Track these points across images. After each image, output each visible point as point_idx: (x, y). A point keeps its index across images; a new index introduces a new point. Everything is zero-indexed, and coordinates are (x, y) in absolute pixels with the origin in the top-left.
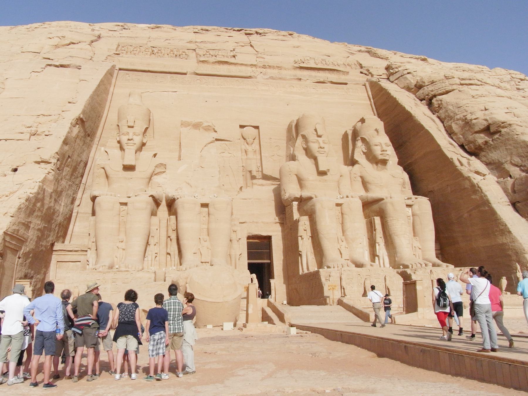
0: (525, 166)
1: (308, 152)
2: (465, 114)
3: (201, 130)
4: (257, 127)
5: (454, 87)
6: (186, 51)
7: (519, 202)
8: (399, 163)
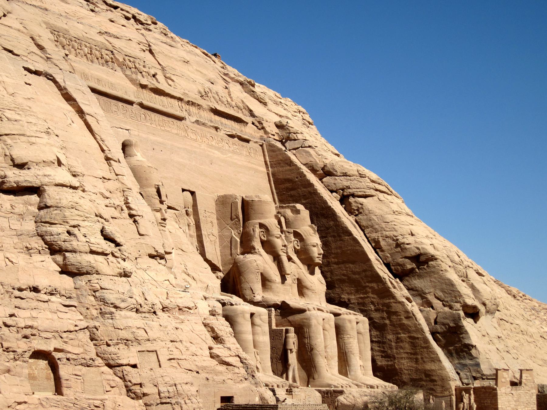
0: (447, 302)
4: (193, 193)
5: (373, 192)
7: (439, 333)
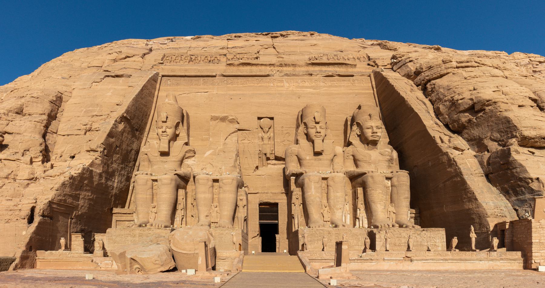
3: (227, 122)
4: (272, 119)
6: (218, 57)
8: (390, 143)
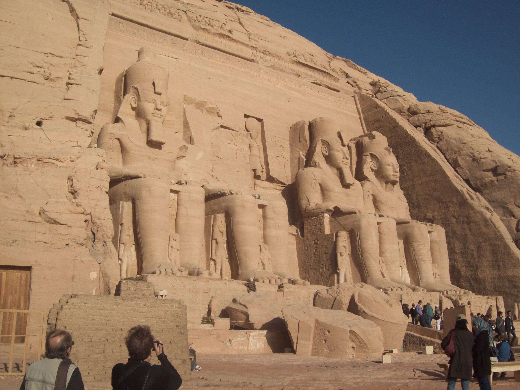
1: (329, 159)
2: (472, 151)
3: (204, 111)
4: (260, 120)
5: (453, 122)
